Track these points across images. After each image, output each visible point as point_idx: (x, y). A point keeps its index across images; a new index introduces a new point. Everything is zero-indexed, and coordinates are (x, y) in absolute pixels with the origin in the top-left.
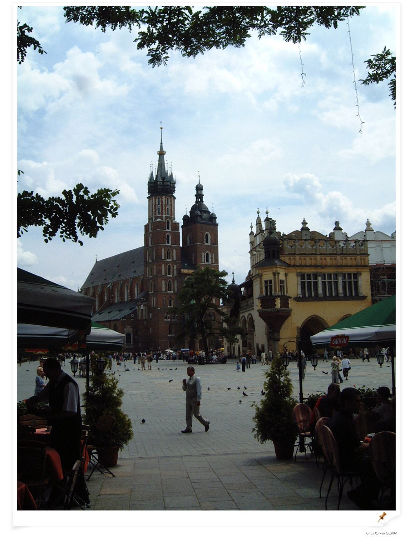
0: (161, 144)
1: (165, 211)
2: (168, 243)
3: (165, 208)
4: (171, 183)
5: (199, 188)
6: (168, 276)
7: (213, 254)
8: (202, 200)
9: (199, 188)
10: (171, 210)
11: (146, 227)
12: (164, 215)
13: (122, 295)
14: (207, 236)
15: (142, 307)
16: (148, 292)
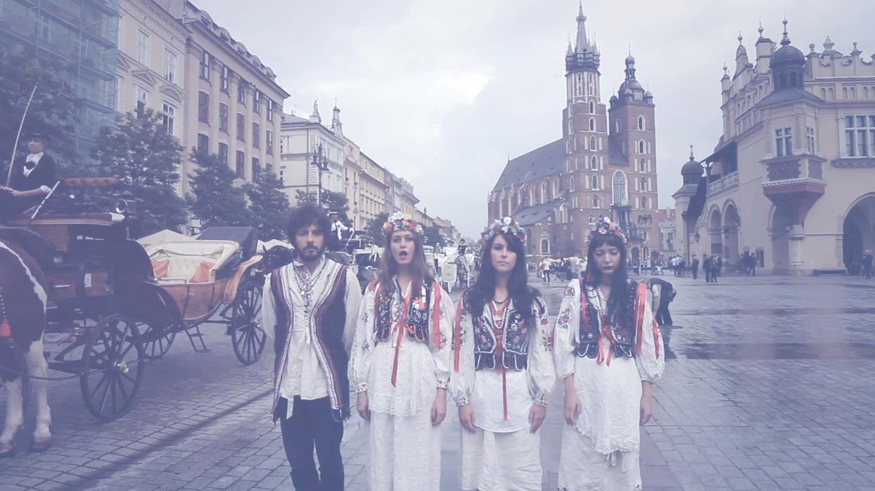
0: (581, 7)
1: (588, 91)
2: (592, 129)
3: (588, 86)
4: (594, 55)
5: (629, 62)
6: (593, 170)
7: (649, 143)
8: (633, 77)
9: (629, 62)
10: (595, 90)
11: (565, 111)
12: (586, 95)
13: (537, 196)
14: (641, 119)
15: (561, 208)
16: (569, 190)
